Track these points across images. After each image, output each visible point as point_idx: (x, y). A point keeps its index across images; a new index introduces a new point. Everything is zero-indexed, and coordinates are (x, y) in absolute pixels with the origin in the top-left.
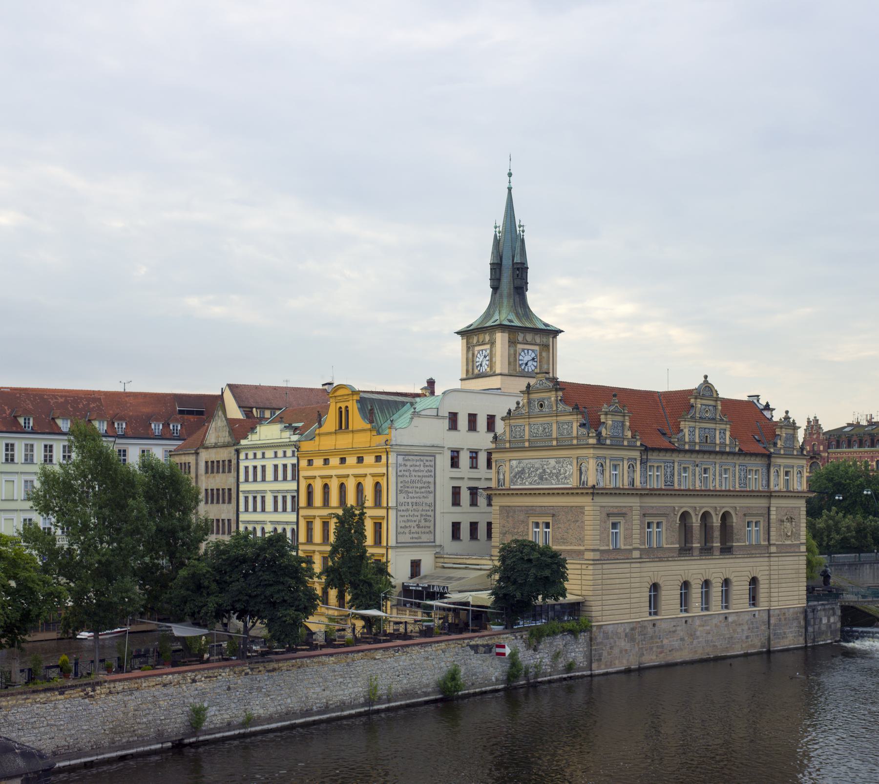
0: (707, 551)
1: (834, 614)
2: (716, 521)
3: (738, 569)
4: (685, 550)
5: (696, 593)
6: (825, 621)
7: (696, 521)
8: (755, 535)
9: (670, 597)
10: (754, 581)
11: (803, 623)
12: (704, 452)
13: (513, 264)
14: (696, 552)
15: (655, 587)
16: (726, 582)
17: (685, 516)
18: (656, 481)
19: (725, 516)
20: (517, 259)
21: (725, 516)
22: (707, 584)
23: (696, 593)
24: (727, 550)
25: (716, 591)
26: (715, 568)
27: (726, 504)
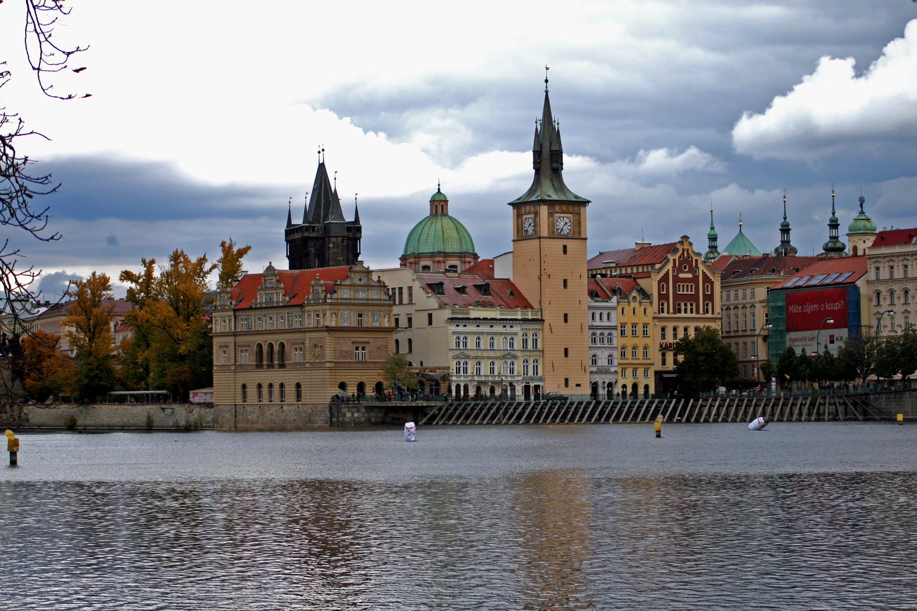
0: (271, 366)
1: (358, 411)
2: (276, 348)
3: (289, 378)
4: (259, 366)
5: (265, 390)
6: (349, 415)
7: (265, 349)
8: (295, 356)
9: (252, 392)
10: (298, 385)
11: (328, 414)
12: (268, 308)
13: (551, 151)
14: (265, 367)
15: (244, 386)
16: (282, 385)
17: (260, 346)
18: (242, 326)
19: (282, 345)
20: (554, 148)
21: (282, 345)
22: (271, 386)
23: (265, 390)
24: (282, 366)
25: (276, 390)
26: (275, 376)
27: (282, 338)
